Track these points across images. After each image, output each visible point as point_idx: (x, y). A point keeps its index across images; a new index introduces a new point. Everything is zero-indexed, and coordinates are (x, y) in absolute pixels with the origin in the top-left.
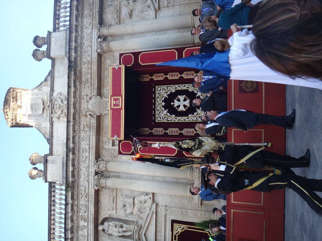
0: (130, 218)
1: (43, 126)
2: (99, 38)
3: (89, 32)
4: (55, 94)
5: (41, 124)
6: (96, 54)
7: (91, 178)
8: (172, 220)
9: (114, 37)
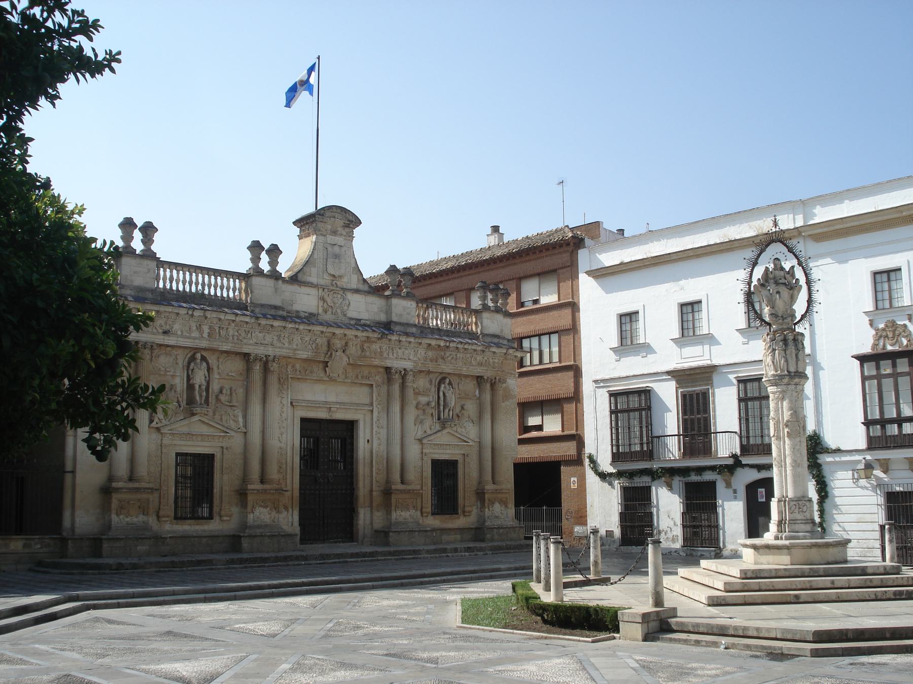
0: (212, 400)
1: (313, 269)
2: (405, 370)
3: (411, 357)
4: (350, 296)
5: (315, 267)
6: (389, 365)
7: (261, 351)
8: (213, 455)
9: (403, 386)
